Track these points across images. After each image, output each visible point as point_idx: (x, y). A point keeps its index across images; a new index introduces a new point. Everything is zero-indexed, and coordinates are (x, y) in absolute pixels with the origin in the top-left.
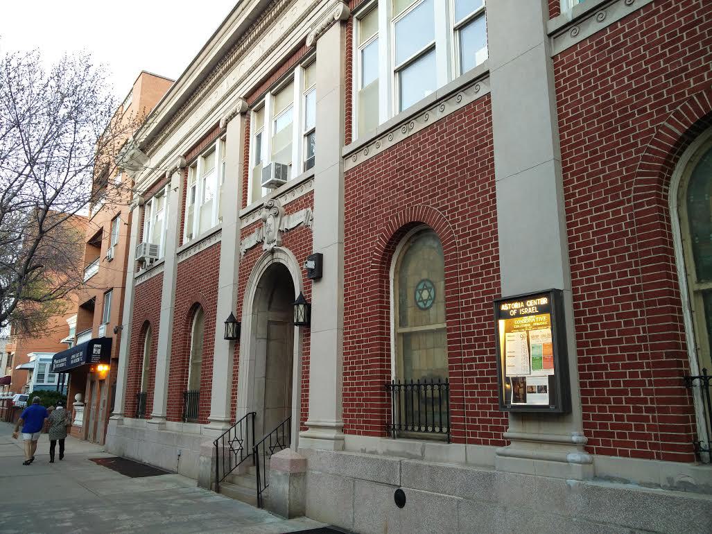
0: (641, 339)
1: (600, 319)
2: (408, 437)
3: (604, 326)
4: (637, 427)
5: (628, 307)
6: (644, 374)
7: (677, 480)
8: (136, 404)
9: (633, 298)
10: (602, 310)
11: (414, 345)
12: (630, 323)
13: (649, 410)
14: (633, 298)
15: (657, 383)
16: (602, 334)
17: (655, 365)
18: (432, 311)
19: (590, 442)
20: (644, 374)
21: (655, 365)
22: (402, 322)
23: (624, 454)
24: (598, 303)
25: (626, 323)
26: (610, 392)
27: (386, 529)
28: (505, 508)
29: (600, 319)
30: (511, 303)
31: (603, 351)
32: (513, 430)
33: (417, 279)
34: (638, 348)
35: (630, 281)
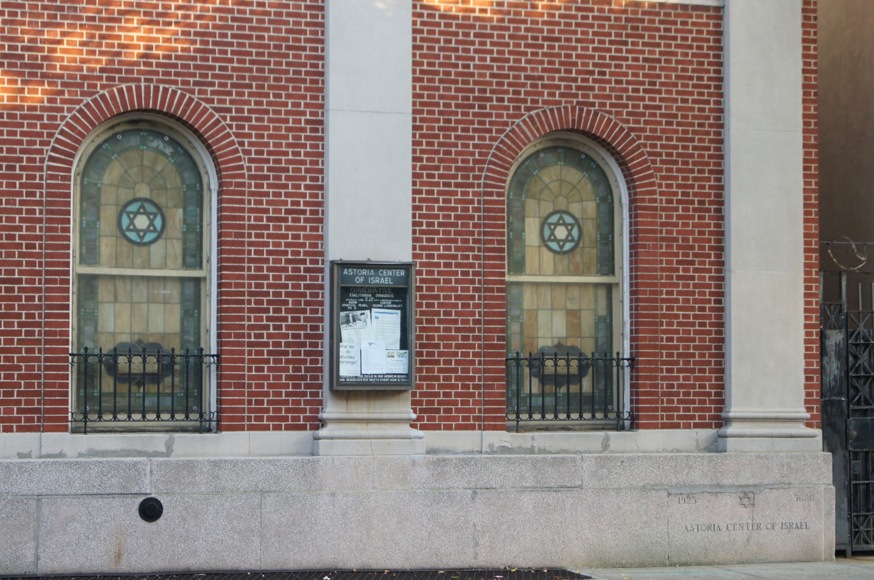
0: (477, 322)
1: (437, 297)
2: (95, 431)
3: (440, 305)
4: (463, 403)
5: (468, 290)
6: (475, 355)
7: (496, 445)
8: (814, 371)
9: (472, 282)
10: (441, 289)
11: (104, 291)
12: (468, 306)
13: (476, 387)
14: (472, 282)
15: (486, 363)
16: (437, 313)
17: (487, 346)
18: (157, 249)
19: (419, 419)
20: (475, 355)
21: (487, 346)
22: (90, 254)
23: (448, 428)
24: (437, 281)
25: (463, 305)
26: (441, 370)
27: (119, 556)
28: (333, 495)
29: (437, 297)
30: (358, 268)
31: (437, 330)
32: (331, 409)
33: (125, 195)
34: (472, 330)
35: (472, 266)
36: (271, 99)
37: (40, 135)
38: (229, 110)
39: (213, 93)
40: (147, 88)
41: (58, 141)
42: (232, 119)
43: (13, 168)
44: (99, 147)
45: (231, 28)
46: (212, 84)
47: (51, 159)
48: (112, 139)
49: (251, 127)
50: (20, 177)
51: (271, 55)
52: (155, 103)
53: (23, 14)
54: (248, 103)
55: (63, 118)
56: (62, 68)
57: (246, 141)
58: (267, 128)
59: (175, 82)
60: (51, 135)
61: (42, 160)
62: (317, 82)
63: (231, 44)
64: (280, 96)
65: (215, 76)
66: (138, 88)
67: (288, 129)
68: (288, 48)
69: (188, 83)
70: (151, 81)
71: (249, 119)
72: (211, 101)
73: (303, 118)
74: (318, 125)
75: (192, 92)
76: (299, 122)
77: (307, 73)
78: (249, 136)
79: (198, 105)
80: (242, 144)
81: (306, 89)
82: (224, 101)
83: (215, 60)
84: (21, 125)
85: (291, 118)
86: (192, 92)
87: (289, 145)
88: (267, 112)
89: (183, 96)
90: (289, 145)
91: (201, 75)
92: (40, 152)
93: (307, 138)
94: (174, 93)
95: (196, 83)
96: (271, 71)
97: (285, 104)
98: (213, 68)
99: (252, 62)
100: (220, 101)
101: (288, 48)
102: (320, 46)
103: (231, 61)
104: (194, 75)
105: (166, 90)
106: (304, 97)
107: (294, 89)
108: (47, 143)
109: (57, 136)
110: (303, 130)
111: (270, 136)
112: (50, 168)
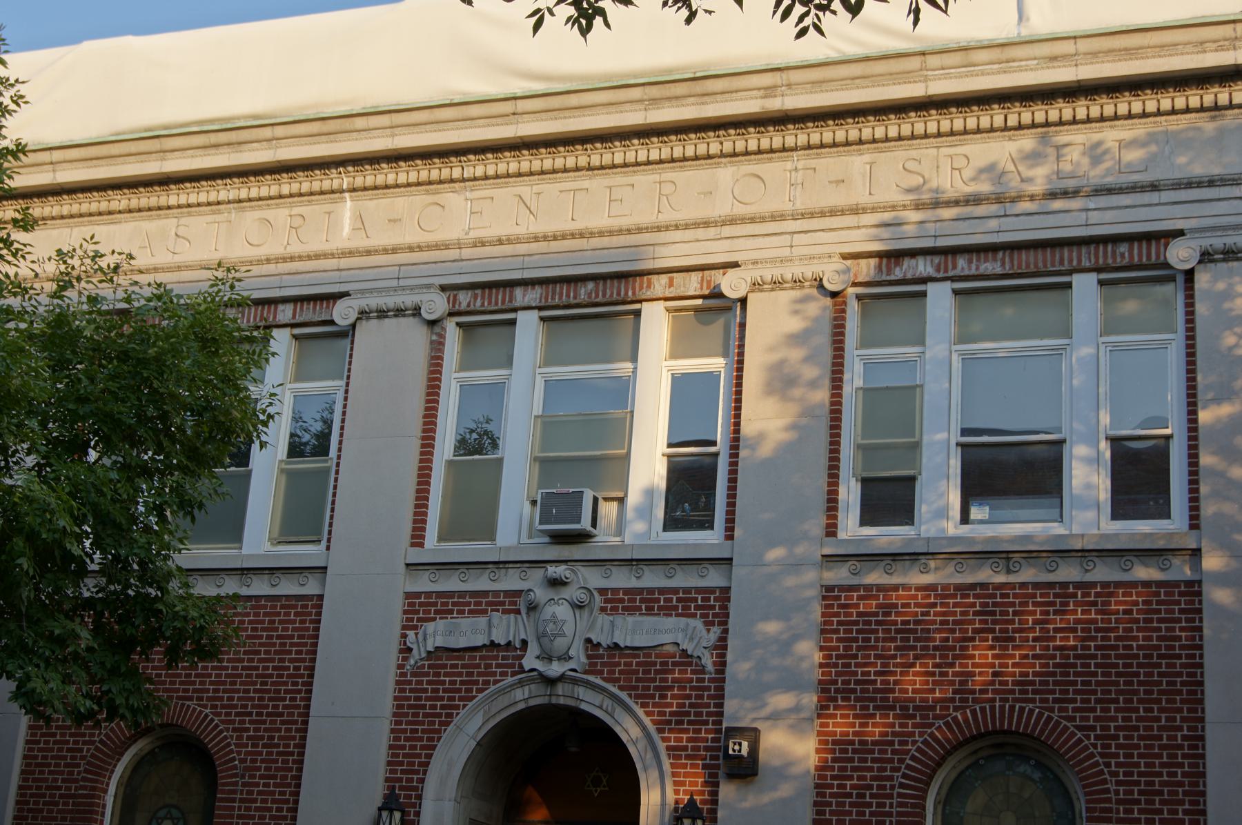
36: (1142, 713)
37: (891, 761)
38: (1093, 728)
39: (1075, 710)
40: (1002, 708)
41: (908, 767)
42: (1097, 737)
43: (864, 796)
44: (962, 772)
45: (1094, 639)
46: (1074, 701)
47: (902, 786)
48: (974, 765)
49: (1118, 746)
50: (870, 805)
51: (1140, 665)
52: (1010, 724)
53: (877, 640)
54: (1115, 719)
55: (914, 742)
56: (914, 691)
57: (1113, 761)
58: (1137, 747)
59: (1033, 701)
60: (901, 761)
61: (892, 787)
62: (1195, 692)
63: (1094, 657)
64: (1152, 710)
65: (1076, 692)
66: (993, 708)
67: (1162, 747)
68: (1160, 656)
69: (1047, 700)
70: (1007, 700)
71: (1116, 737)
72: (1073, 719)
73: (1179, 734)
74: (1197, 740)
75: (1052, 710)
76: (1175, 738)
77: (1183, 684)
78: (1117, 755)
79: (1058, 723)
80: (1108, 765)
81: (1182, 701)
82: (1087, 719)
83: (1077, 674)
84: (872, 752)
85: (1165, 735)
86: (1052, 710)
87: (1163, 765)
88: (1137, 728)
89: (1040, 715)
90: (1163, 765)
91: (1061, 692)
92: (891, 778)
93: (1184, 756)
94: (1031, 711)
95: (1055, 701)
96: (1140, 683)
97: (1158, 719)
98: (1074, 683)
99: (1118, 674)
100: (1082, 719)
101: (1160, 656)
102: (1198, 652)
103: (1095, 674)
104: (1053, 692)
105: (1022, 709)
106: (1180, 710)
107: (1168, 701)
108: (898, 770)
109: (908, 761)
110: (1181, 747)
111: (1140, 756)
112: (900, 795)
